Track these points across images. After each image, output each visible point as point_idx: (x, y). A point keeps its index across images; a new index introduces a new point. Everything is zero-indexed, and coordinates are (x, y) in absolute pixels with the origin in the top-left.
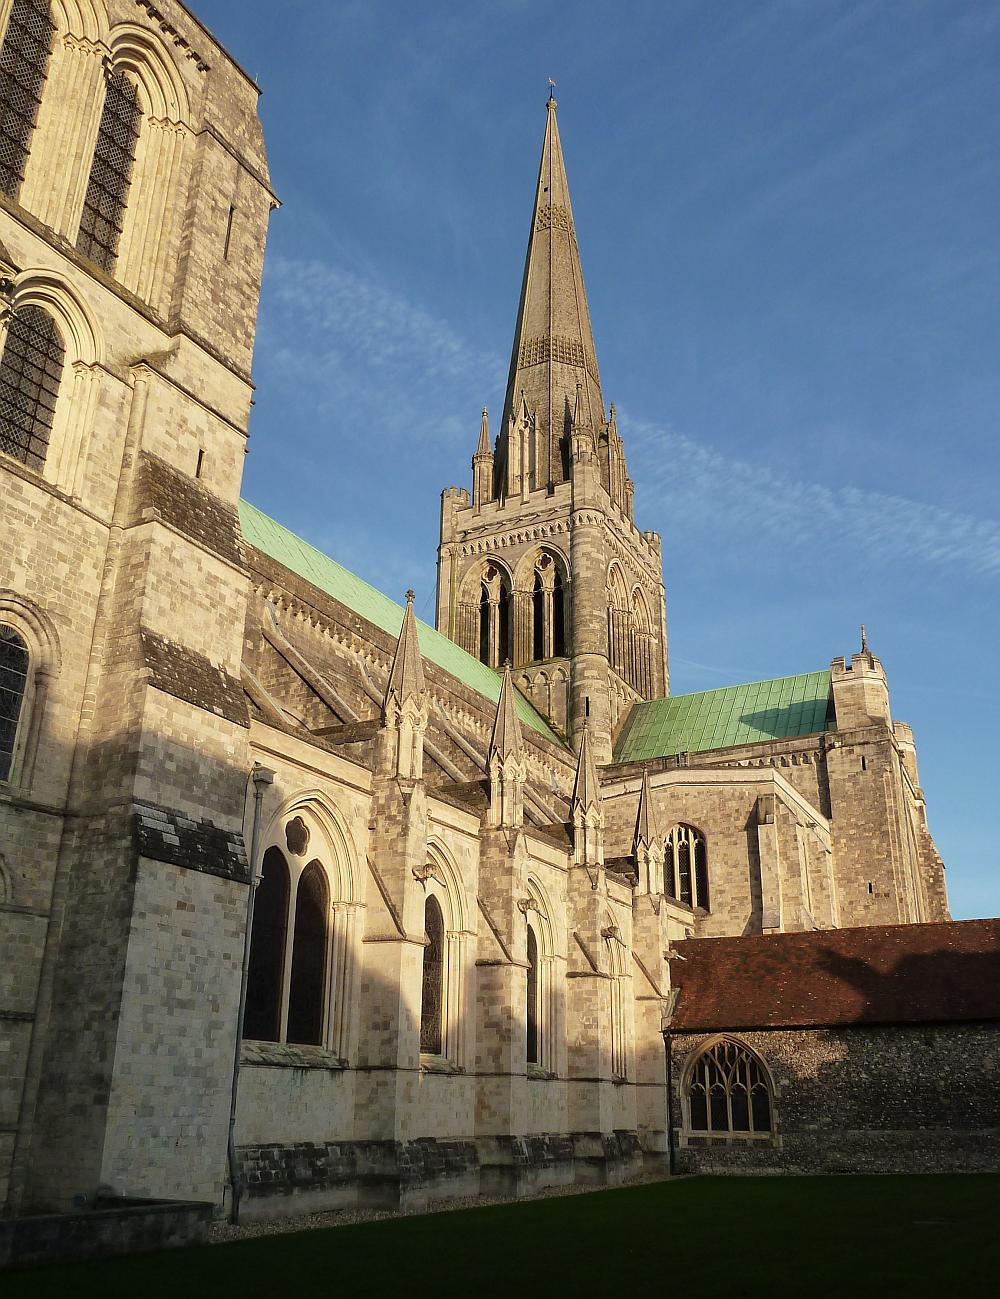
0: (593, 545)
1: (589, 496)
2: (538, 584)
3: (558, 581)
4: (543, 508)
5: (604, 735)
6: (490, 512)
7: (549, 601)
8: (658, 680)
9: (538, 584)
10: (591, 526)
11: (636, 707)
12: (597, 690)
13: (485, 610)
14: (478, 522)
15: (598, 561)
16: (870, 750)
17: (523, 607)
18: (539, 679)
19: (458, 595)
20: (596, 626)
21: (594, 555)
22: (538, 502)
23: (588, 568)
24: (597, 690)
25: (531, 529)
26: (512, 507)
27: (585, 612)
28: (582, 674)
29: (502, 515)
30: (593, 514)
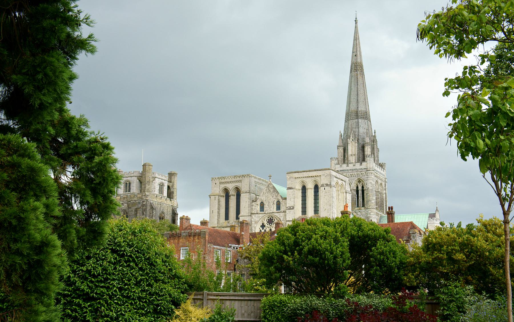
2: (357, 187)
3: (363, 187)
7: (360, 192)
8: (385, 206)
9: (357, 187)
12: (374, 218)
14: (341, 169)
21: (373, 183)
22: (358, 166)
23: (371, 187)
24: (374, 218)
28: (370, 214)
29: (348, 168)
30: (372, 172)
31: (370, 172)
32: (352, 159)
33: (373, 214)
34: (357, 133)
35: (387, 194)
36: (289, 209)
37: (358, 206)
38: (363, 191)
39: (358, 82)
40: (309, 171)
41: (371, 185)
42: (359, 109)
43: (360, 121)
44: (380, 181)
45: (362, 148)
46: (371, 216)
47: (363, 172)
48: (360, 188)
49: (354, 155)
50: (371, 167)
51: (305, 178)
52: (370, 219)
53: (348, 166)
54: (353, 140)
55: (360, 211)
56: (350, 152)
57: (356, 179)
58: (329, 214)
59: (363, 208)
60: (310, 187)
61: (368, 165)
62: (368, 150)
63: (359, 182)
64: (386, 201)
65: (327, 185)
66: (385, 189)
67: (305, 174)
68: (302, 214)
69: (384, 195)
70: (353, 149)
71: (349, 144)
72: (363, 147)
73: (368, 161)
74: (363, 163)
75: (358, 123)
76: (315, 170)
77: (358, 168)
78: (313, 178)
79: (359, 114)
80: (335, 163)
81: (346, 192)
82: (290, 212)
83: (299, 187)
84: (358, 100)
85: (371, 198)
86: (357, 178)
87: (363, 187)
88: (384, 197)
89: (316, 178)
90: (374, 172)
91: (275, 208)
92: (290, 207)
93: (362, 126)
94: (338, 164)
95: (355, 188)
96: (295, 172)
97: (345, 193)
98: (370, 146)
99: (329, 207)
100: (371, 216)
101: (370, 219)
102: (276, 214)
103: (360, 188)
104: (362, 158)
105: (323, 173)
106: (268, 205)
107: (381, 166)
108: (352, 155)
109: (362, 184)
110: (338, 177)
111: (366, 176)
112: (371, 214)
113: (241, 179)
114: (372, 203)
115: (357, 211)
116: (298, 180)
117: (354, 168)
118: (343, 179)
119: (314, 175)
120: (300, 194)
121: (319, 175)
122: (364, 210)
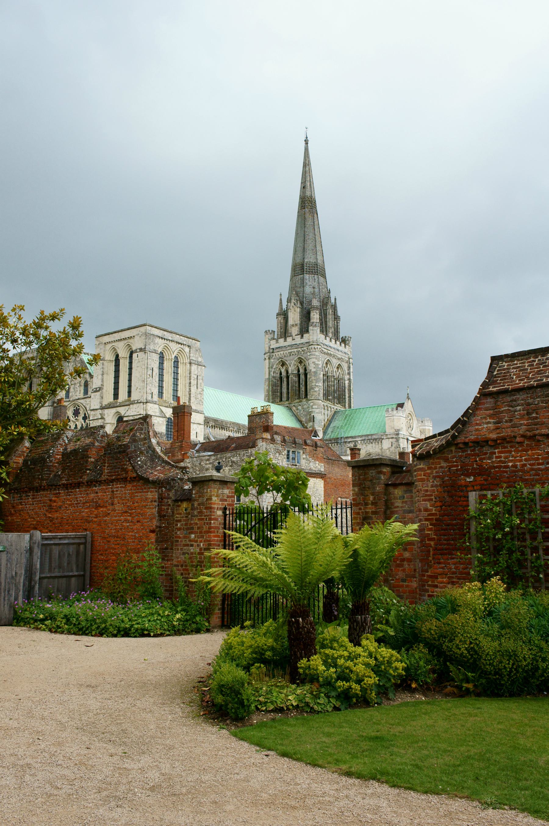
0: (316, 358)
1: (315, 340)
3: (305, 370)
4: (300, 342)
5: (319, 428)
6: (281, 341)
7: (302, 377)
9: (299, 371)
10: (315, 351)
11: (336, 413)
12: (317, 413)
13: (281, 378)
14: (278, 345)
15: (318, 364)
16: (394, 440)
17: (293, 378)
18: (300, 407)
19: (272, 373)
20: (317, 389)
21: (317, 362)
22: (298, 340)
24: (317, 413)
25: (295, 350)
26: (289, 339)
28: (312, 407)
29: (286, 344)
30: (316, 347)
31: (313, 346)
32: (295, 331)
33: (316, 407)
34: (301, 295)
35: (352, 381)
36: (96, 391)
37: (299, 398)
38: (306, 375)
39: (306, 223)
40: (122, 331)
41: (314, 366)
42: (306, 260)
43: (307, 276)
44: (335, 362)
45: (306, 317)
46: (313, 410)
47: (305, 348)
48: (302, 371)
49: (296, 325)
50: (315, 340)
51: (117, 343)
52: (312, 415)
53: (285, 340)
54: (295, 304)
55: (300, 403)
56: (291, 322)
57: (295, 359)
58: (141, 394)
59: (304, 400)
60: (123, 354)
61: (311, 337)
62: (315, 316)
63: (301, 362)
64: (350, 391)
65: (141, 350)
66: (349, 374)
67: (117, 336)
68: (114, 399)
69: (347, 382)
70: (294, 317)
71: (289, 310)
72: (309, 313)
73: (311, 331)
74: (304, 335)
75: (303, 280)
76: (129, 329)
77: (298, 343)
78: (125, 342)
79: (305, 267)
80: (270, 338)
81: (190, 363)
82: (95, 396)
83: (110, 356)
84: (304, 248)
85: (313, 384)
86: (297, 358)
87: (305, 370)
88: (347, 385)
89: (129, 340)
90: (319, 347)
91: (82, 391)
92: (96, 388)
93: (309, 283)
94: (274, 339)
95: (296, 372)
96: (106, 335)
97: (188, 365)
98: (317, 311)
99: (142, 384)
100: (313, 410)
101: (312, 415)
102: (82, 401)
103: (302, 371)
104: (304, 330)
105: (138, 332)
106: (74, 388)
107: (344, 341)
108: (293, 325)
109: (305, 365)
110: (170, 338)
111: (309, 354)
112: (314, 407)
114: (316, 391)
115: (297, 404)
116: (109, 346)
117: (293, 343)
118: (185, 343)
119: (127, 336)
120: (113, 368)
121: (132, 335)
122: (305, 403)
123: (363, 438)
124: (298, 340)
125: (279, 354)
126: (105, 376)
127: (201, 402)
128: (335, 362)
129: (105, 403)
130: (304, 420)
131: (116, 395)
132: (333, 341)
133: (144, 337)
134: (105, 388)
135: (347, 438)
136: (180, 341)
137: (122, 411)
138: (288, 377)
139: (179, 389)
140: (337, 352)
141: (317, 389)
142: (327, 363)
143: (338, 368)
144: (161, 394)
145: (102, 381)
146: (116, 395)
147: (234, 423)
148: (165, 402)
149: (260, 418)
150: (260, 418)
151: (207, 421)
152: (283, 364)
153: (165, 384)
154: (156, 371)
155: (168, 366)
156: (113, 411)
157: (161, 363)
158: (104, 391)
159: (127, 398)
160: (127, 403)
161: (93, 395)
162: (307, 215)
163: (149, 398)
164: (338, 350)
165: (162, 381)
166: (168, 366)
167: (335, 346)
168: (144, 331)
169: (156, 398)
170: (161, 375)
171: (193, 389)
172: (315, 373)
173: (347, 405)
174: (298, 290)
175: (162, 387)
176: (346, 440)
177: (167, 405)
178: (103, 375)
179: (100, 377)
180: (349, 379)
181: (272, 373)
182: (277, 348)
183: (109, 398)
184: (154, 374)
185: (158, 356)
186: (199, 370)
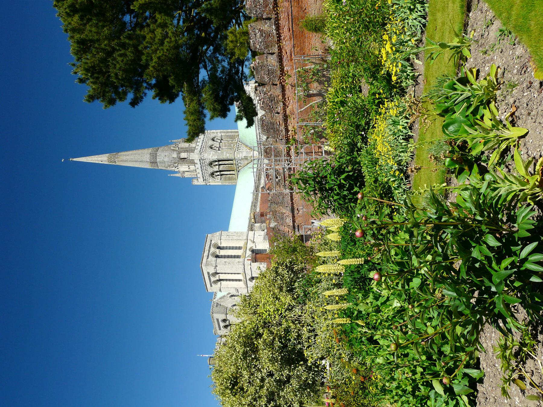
0: (209, 155)
7: (220, 163)
17: (222, 168)
19: (218, 181)
27: (225, 157)
30: (202, 156)
31: (202, 158)
32: (192, 167)
33: (238, 155)
38: (219, 161)
42: (148, 160)
43: (158, 160)
44: (211, 143)
56: (187, 169)
62: (183, 155)
66: (217, 133)
73: (193, 159)
75: (160, 162)
77: (200, 166)
87: (216, 161)
90: (202, 154)
93: (163, 159)
104: (192, 162)
108: (189, 168)
110: (208, 252)
113: (215, 319)
123: (257, 129)
124: (198, 166)
125: (207, 176)
126: (229, 286)
127: (242, 233)
128: (211, 143)
129: (244, 286)
130: (246, 162)
131: (240, 280)
132: (198, 143)
133: (208, 267)
134: (235, 286)
135: (257, 138)
136: (209, 246)
137: (248, 277)
138: (221, 171)
139: (235, 246)
140: (204, 141)
141: (228, 155)
142: (212, 148)
143: (214, 140)
144: (238, 257)
145: (232, 288)
146: (240, 280)
147: (251, 209)
148: (243, 254)
149: (257, 218)
150: (257, 218)
151: (251, 228)
152: (212, 174)
153: (233, 254)
154: (226, 260)
155: (222, 253)
156: (248, 282)
157: (222, 257)
158: (237, 287)
159: (241, 275)
160: (244, 275)
161: (240, 293)
162: (119, 159)
163: (241, 263)
164: (203, 141)
165: (231, 256)
166: (222, 253)
167: (201, 142)
168: (205, 267)
169: (241, 260)
170: (228, 257)
171: (235, 238)
172: (218, 156)
173: (236, 134)
174: (166, 165)
175: (235, 256)
176: (259, 139)
177: (244, 253)
178: (228, 288)
179: (229, 289)
180: (220, 132)
181: (218, 181)
182: (203, 178)
183: (241, 284)
184: (228, 261)
185: (218, 259)
186: (224, 234)
